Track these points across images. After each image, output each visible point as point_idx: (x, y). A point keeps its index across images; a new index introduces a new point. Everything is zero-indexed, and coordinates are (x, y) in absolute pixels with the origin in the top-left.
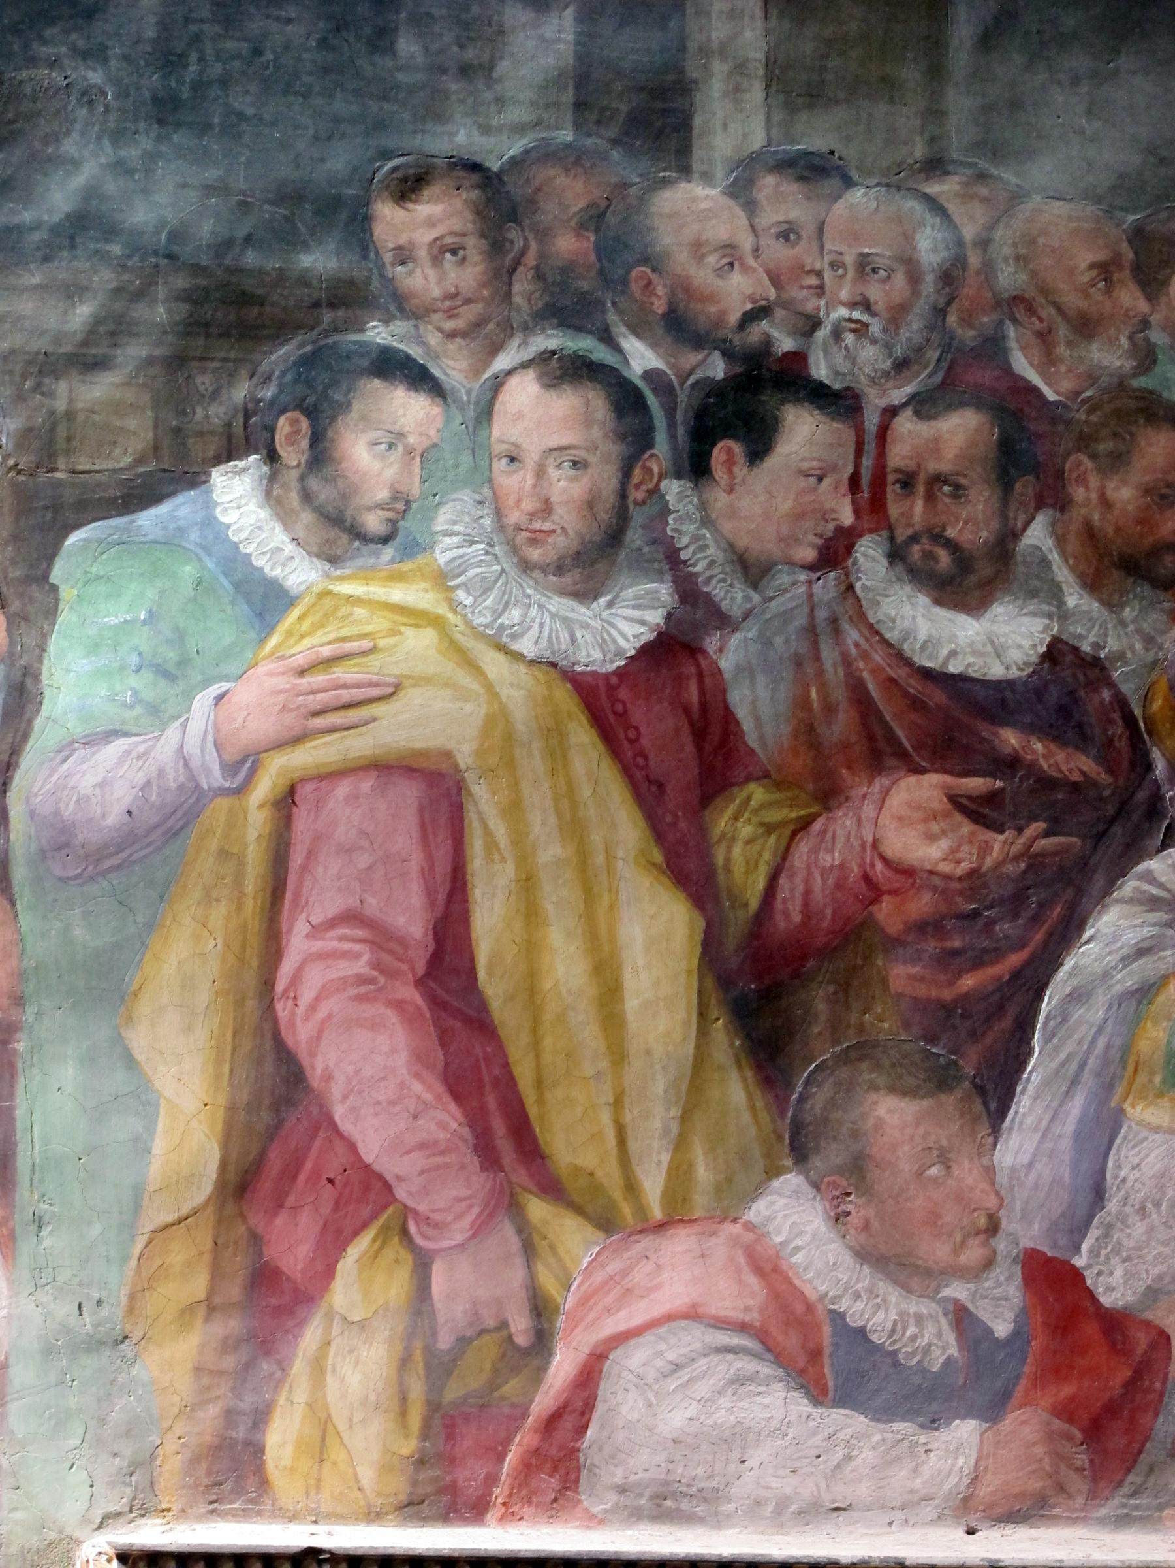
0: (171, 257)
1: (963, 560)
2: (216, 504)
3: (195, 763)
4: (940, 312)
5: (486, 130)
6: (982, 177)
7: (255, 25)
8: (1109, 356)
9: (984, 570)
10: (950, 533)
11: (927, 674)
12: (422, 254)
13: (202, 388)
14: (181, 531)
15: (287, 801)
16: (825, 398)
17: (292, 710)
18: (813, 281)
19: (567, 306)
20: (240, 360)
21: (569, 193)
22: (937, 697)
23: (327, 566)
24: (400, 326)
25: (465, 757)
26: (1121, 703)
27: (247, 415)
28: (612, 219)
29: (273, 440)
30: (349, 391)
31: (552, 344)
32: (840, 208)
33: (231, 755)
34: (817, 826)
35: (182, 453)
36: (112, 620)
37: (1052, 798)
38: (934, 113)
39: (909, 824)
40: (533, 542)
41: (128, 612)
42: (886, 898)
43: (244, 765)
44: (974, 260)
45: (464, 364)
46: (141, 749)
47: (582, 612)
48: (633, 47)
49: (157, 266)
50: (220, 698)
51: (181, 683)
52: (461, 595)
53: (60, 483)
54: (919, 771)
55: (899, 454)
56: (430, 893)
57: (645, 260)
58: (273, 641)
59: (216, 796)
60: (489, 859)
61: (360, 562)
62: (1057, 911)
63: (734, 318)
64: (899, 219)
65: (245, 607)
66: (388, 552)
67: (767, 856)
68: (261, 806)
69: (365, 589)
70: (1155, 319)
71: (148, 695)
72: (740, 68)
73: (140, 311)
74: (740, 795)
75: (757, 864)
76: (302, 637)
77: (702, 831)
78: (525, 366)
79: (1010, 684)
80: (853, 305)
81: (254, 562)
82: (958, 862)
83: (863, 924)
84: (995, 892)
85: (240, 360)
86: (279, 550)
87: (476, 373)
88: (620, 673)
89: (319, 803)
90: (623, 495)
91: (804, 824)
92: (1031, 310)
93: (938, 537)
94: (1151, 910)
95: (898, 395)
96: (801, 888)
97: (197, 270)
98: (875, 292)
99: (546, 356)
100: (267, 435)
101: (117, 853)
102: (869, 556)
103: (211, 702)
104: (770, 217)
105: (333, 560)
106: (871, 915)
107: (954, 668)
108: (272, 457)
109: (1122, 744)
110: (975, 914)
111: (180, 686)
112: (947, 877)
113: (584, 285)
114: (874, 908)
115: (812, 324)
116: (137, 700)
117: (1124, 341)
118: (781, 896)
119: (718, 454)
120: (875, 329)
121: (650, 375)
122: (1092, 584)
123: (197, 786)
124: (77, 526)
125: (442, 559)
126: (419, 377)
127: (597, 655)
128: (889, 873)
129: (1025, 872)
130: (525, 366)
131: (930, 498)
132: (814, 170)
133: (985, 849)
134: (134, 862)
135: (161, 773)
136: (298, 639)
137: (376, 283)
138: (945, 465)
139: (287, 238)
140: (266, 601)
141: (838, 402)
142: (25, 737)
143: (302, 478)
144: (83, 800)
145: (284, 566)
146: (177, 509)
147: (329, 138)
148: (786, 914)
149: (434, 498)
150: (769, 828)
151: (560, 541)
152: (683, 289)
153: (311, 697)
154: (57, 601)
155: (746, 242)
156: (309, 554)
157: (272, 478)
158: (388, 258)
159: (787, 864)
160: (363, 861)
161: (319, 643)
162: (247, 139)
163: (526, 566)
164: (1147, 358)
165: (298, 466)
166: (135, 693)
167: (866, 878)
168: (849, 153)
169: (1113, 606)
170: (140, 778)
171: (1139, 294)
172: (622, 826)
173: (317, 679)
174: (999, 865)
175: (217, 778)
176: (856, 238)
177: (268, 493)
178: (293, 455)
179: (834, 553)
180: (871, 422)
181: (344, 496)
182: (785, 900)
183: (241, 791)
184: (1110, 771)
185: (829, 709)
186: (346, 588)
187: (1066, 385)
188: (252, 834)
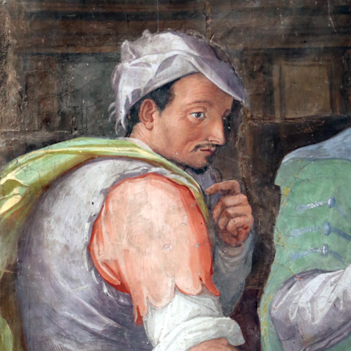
36: (313, 206)
41: (321, 200)
46: (333, 279)
53: (277, 127)
71: (334, 248)
73: (317, 21)
101: (322, 341)
116: (329, 252)
124: (289, 151)
134: (333, 346)
142: (266, 275)
144: (301, 311)
154: (280, 195)
166: (327, 246)
170: (333, 298)
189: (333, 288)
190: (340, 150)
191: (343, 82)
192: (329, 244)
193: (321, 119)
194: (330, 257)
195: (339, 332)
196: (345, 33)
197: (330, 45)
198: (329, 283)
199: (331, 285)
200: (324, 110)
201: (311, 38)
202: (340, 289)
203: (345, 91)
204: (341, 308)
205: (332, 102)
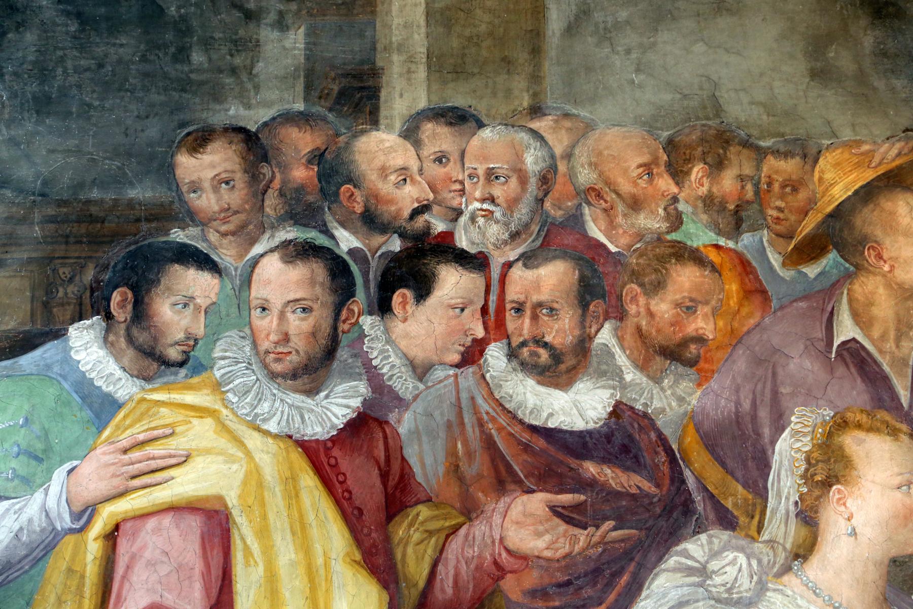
0: (43, 195)
1: (557, 356)
2: (71, 348)
3: (53, 515)
4: (540, 201)
5: (248, 106)
6: (567, 115)
7: (99, 51)
8: (652, 222)
9: (570, 361)
10: (548, 339)
11: (534, 429)
12: (207, 185)
13: (63, 276)
14: (48, 367)
15: (112, 536)
16: (464, 259)
17: (119, 476)
18: (458, 187)
19: (301, 211)
20: (90, 257)
21: (301, 142)
22: (540, 443)
23: (143, 383)
24: (193, 231)
25: (232, 500)
26: (662, 439)
27: (92, 291)
28: (328, 156)
29: (109, 306)
30: (159, 273)
31: (290, 236)
32: (475, 142)
33: (77, 508)
34: (463, 531)
35: (49, 316)
37: (622, 507)
38: (536, 78)
39: (526, 526)
40: (278, 360)
42: (509, 576)
43: (85, 514)
44: (562, 167)
45: (233, 252)
46: (17, 507)
47: (309, 402)
48: (342, 51)
49: (34, 201)
50: (70, 472)
51: (45, 463)
52: (230, 395)
54: (531, 491)
55: (513, 293)
56: (207, 589)
57: (350, 180)
58: (107, 433)
59: (66, 534)
60: (247, 564)
61: (165, 379)
62: (625, 578)
63: (406, 213)
64: (512, 145)
65: (89, 412)
66: (183, 372)
67: (430, 551)
68: (96, 539)
69: (168, 396)
70: (681, 196)
71: (22, 471)
72: (411, 60)
74: (413, 512)
75: (423, 558)
76: (126, 429)
77: (387, 539)
78: (272, 251)
79: (590, 433)
80: (483, 200)
81: (96, 383)
82: (557, 550)
83: (493, 592)
84: (582, 569)
85: (90, 257)
86: (112, 374)
87: (241, 256)
88: (333, 440)
89: (135, 534)
90: (335, 328)
91: (455, 529)
92: (599, 196)
93: (539, 342)
94: (687, 576)
95: (512, 256)
96: (452, 572)
97: (61, 203)
98: (498, 191)
99: (286, 244)
100: (104, 303)
102: (495, 355)
103: (65, 474)
104: (430, 149)
105: (147, 379)
106: (498, 586)
107: (551, 424)
108: (109, 317)
109: (665, 469)
110: (568, 583)
111: (45, 466)
112: (548, 560)
113: (311, 198)
114: (501, 583)
115: (459, 213)
116: (16, 475)
117: (661, 211)
118: (439, 577)
119: (396, 299)
120: (498, 214)
121: (352, 252)
122: (642, 366)
123: (54, 529)
125: (218, 374)
126: (205, 262)
127: (318, 429)
128: (512, 560)
129: (601, 554)
130: (272, 251)
131: (535, 317)
132: (460, 119)
133: (574, 539)
135: (30, 521)
136: (124, 429)
137: (177, 205)
138: (544, 297)
139: (119, 180)
140: (102, 408)
141: (474, 261)
143: (128, 329)
145: (115, 384)
146: (46, 352)
147: (147, 117)
148: (443, 590)
149: (214, 336)
150: (430, 533)
151: (294, 358)
152: (374, 197)
153: (131, 467)
155: (414, 165)
156: (132, 376)
157: (108, 330)
158: (184, 189)
159: (444, 556)
160: (164, 570)
161: (138, 432)
162: (94, 120)
163: (273, 376)
164: (676, 221)
165: (125, 321)
166: (14, 470)
167: (495, 563)
168: (480, 107)
169: (657, 380)
170: (16, 527)
171: (671, 181)
172: (333, 537)
173: (135, 455)
174: (584, 550)
175: (67, 522)
176: (485, 159)
177: (105, 339)
178: (121, 314)
179: (472, 355)
180: (495, 273)
181: (155, 339)
182: (442, 580)
183: (81, 530)
184: (658, 486)
185: (470, 455)
186: (156, 396)
187: (624, 241)
188: (90, 558)
189: (16, 516)
190: (38, 365)
191: (47, 294)
192: (17, 468)
193: (20, 333)
194: (16, 482)
195: (19, 566)
196: (52, 243)
197: (34, 255)
198: (12, 511)
199: (15, 513)
200: (23, 323)
201: (14, 248)
202: (24, 518)
203: (48, 303)
204: (24, 538)
205: (33, 315)
